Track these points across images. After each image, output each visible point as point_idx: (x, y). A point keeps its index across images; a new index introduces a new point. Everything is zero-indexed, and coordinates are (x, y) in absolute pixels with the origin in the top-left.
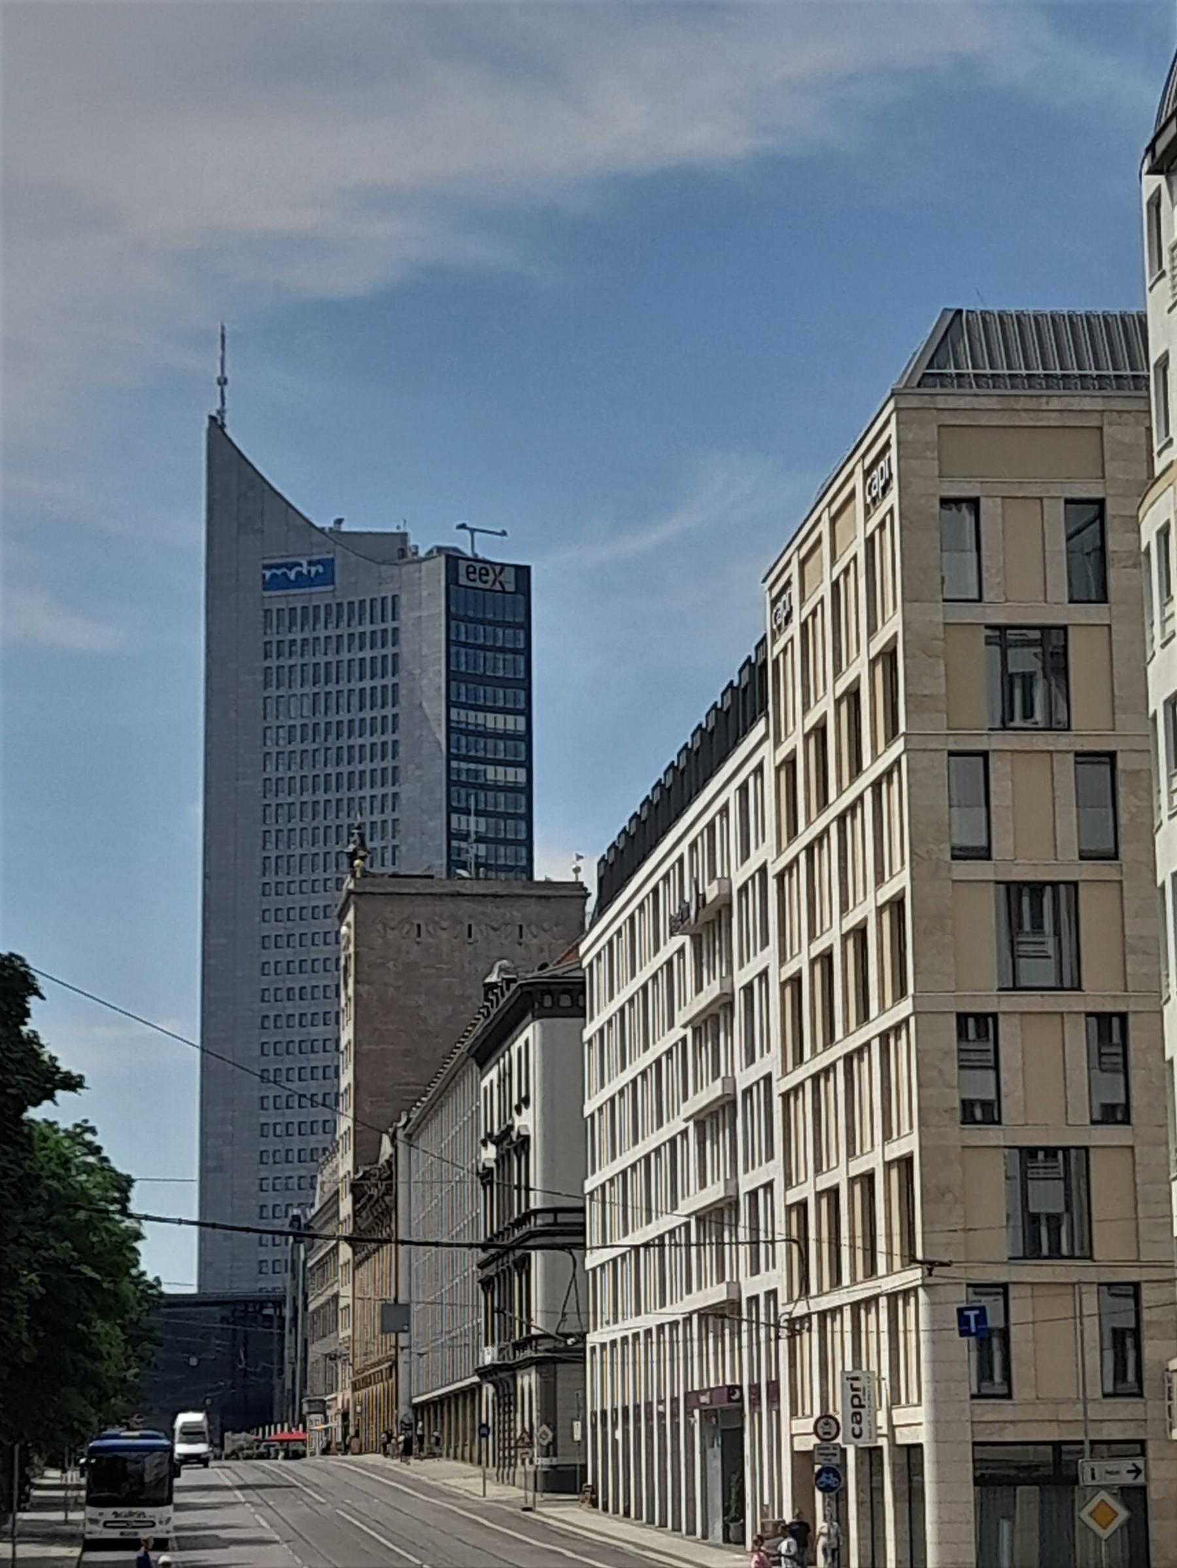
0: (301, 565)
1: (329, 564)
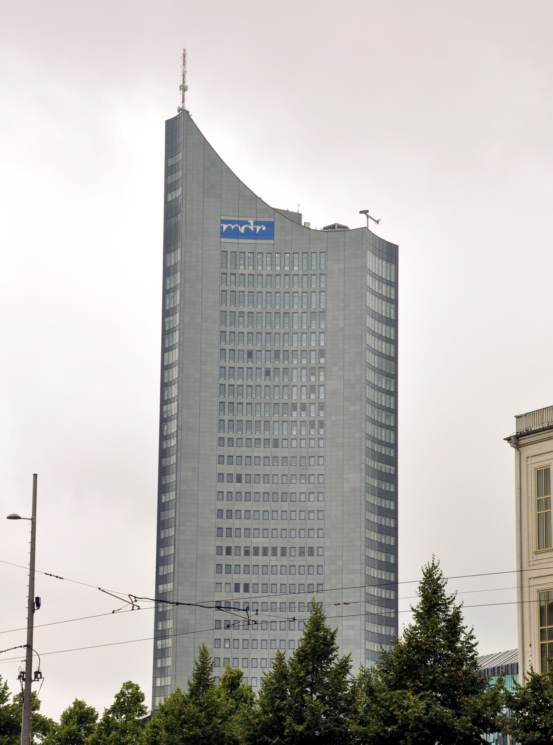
0: (249, 224)
1: (270, 225)
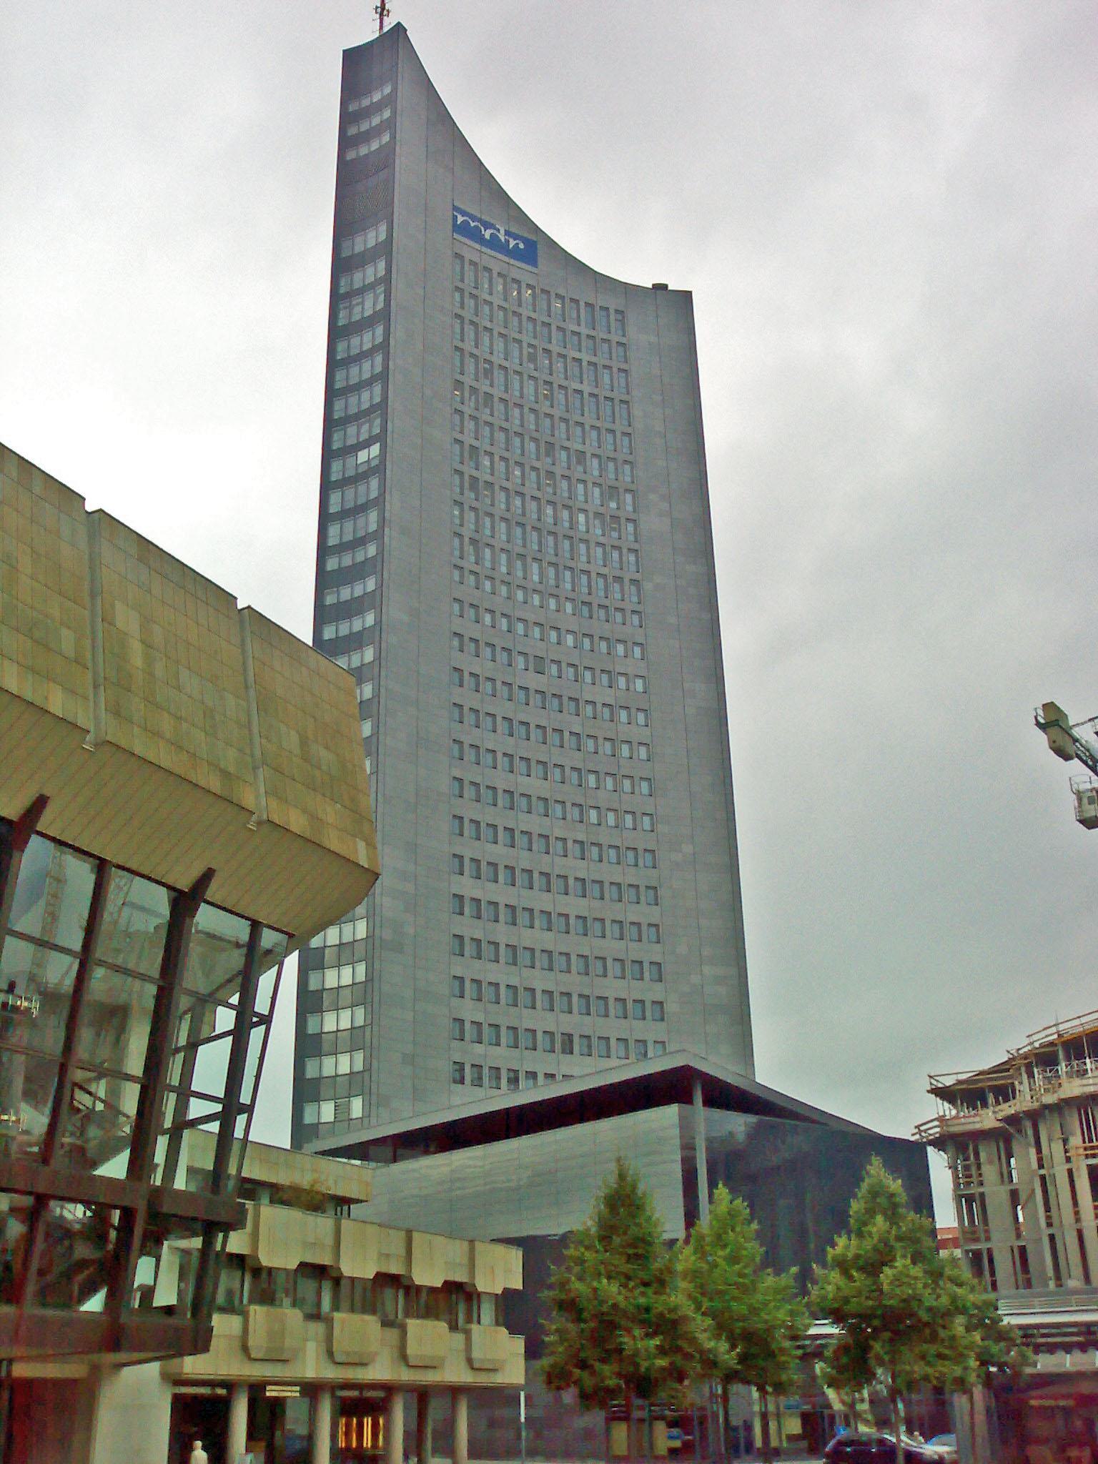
1: (531, 245)
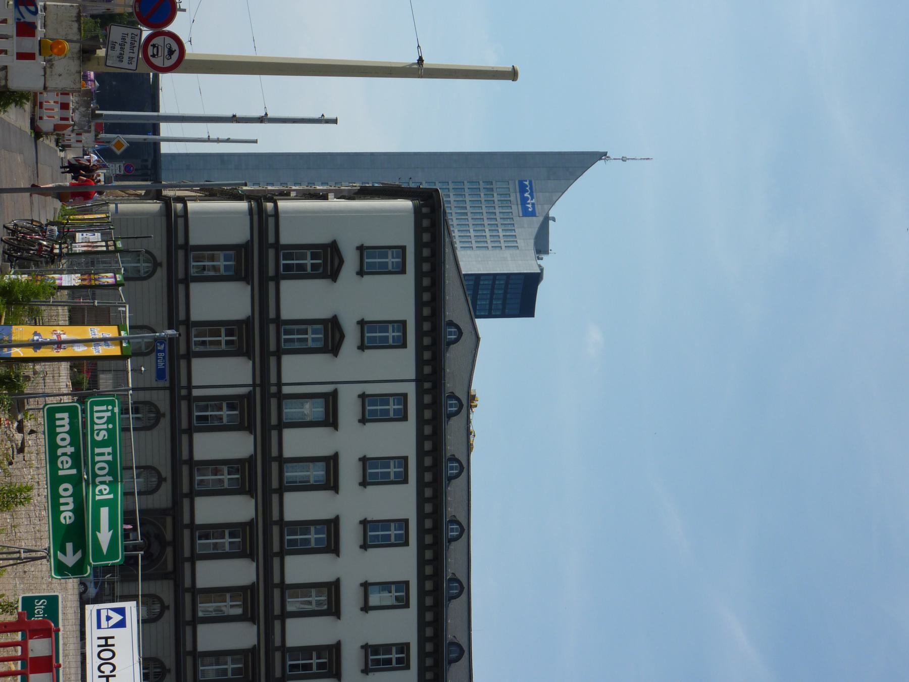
1: (533, 214)
